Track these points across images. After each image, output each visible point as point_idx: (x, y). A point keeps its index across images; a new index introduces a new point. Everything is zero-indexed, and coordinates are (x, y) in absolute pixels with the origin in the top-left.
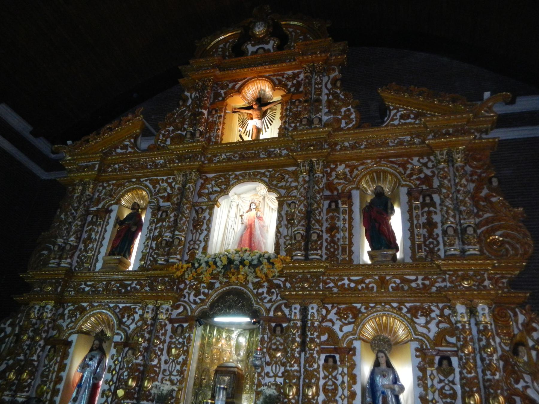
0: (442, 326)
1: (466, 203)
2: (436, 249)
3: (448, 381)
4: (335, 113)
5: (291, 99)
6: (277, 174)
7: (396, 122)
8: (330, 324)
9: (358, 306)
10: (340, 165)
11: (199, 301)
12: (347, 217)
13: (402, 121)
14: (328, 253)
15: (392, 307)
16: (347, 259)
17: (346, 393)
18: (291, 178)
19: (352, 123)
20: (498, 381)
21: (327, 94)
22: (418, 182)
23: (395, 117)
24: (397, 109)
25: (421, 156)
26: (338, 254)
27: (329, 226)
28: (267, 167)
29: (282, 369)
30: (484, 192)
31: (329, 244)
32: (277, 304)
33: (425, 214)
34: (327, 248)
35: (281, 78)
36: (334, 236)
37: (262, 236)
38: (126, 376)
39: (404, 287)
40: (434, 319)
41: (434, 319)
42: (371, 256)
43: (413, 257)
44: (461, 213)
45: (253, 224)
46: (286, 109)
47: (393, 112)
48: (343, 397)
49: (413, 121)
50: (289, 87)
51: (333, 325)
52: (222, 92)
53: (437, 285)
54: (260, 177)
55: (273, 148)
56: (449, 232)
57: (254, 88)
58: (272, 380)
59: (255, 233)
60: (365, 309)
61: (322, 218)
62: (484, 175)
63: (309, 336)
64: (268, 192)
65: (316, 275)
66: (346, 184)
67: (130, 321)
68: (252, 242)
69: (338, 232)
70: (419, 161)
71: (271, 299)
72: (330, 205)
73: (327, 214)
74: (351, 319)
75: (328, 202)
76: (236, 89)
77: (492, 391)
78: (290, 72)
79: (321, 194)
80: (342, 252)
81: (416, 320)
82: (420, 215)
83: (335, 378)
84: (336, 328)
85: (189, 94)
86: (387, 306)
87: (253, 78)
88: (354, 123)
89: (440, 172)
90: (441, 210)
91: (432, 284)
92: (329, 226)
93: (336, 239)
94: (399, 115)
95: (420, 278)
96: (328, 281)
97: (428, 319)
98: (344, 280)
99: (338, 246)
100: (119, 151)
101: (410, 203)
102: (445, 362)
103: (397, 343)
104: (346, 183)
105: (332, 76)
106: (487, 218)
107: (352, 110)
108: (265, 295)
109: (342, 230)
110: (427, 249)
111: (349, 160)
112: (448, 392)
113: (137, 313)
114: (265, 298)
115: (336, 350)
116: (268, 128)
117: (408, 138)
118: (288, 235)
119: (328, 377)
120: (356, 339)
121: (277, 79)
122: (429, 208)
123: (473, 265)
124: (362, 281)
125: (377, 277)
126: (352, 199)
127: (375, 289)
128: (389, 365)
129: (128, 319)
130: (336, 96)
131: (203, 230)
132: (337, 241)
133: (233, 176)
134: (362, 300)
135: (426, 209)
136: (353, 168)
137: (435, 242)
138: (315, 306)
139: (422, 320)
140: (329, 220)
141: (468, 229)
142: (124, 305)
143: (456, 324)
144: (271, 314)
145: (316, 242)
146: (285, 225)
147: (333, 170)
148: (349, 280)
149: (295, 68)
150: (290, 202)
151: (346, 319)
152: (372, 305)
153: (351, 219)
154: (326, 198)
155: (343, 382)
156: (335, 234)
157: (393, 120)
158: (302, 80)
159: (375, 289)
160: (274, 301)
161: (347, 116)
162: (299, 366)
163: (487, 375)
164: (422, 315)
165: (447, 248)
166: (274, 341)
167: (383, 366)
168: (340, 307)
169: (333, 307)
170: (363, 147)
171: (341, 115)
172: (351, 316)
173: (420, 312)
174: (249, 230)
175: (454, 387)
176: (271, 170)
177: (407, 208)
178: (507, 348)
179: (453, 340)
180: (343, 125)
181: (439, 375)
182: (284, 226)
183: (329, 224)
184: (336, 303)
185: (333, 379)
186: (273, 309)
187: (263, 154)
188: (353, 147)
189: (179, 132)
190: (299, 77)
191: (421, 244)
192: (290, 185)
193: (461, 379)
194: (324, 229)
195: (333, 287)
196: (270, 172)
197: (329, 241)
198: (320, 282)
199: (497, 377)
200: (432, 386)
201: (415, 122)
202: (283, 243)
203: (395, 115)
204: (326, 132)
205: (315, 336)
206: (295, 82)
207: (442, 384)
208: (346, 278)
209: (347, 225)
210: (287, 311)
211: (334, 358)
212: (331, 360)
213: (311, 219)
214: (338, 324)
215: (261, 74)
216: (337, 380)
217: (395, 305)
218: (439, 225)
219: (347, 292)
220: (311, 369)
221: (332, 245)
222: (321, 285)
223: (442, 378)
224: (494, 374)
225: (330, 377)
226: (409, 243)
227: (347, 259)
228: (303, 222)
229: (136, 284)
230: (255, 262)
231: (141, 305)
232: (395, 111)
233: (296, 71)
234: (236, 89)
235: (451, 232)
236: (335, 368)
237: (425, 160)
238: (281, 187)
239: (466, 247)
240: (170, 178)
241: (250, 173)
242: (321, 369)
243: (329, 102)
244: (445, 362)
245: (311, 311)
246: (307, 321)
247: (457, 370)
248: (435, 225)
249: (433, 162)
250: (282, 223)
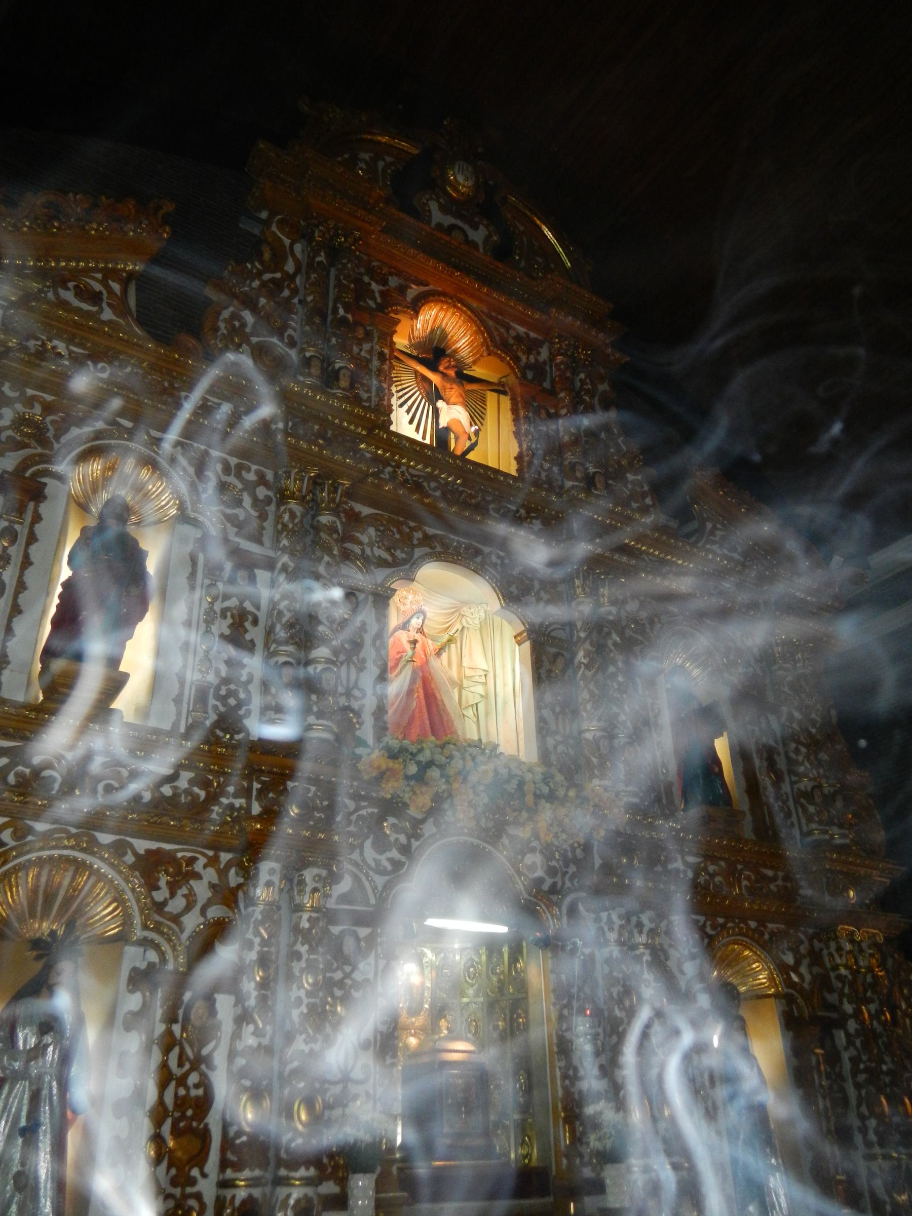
11: (389, 868)
35: (503, 330)
38: (197, 1086)
52: (374, 286)
59: (438, 696)
60: (714, 927)
64: (502, 607)
67: (177, 904)
76: (409, 299)
78: (521, 330)
85: (287, 242)
87: (444, 294)
100: (68, 295)
113: (198, 876)
129: (173, 895)
131: (364, 661)
133: (418, 535)
142: (153, 845)
171: (627, 488)
189: (275, 340)
190: (539, 353)
193: (855, 1072)
206: (532, 359)
215: (462, 296)
229: (191, 782)
231: (211, 853)
233: (533, 335)
234: (409, 299)
240: (249, 470)
247: (846, 1056)
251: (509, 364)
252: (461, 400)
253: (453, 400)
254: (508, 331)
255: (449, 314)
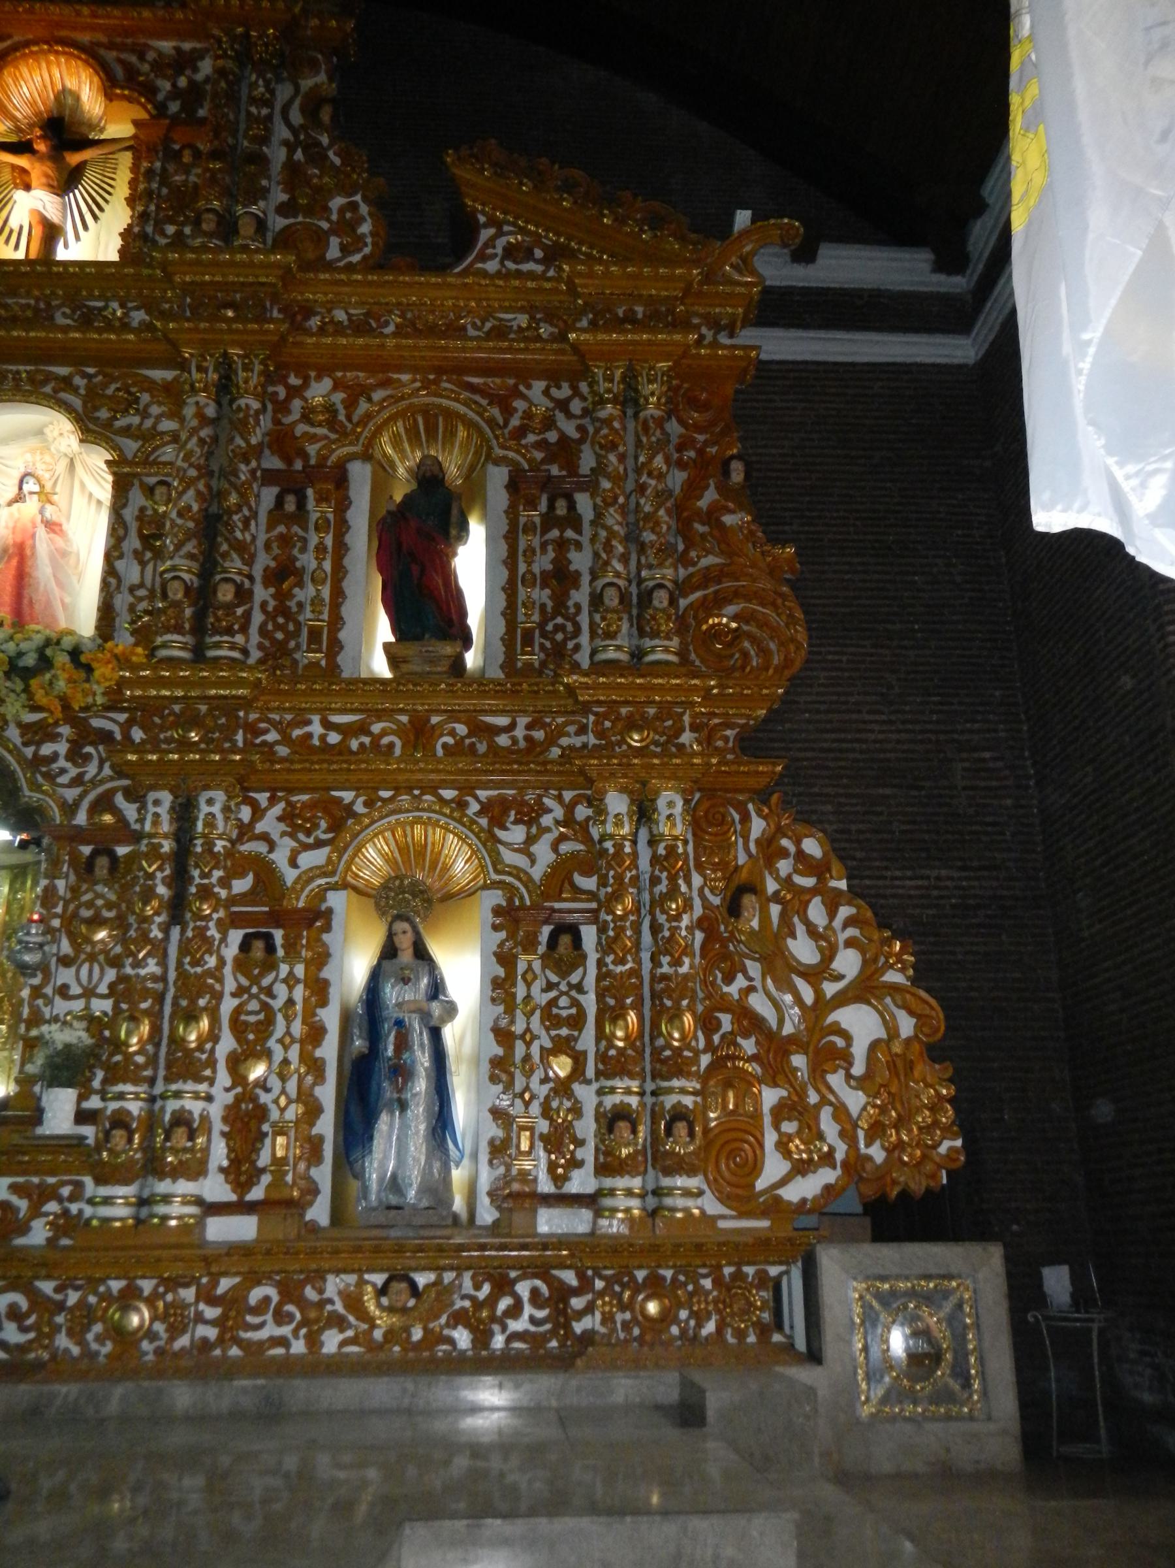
0: (565, 848)
1: (657, 523)
2: (570, 645)
3: (569, 984)
4: (309, 211)
5: (167, 140)
6: (113, 387)
7: (492, 266)
8: (262, 848)
9: (347, 796)
10: (319, 378)
12: (329, 541)
13: (510, 265)
14: (267, 643)
15: (441, 800)
16: (323, 663)
17: (297, 1028)
18: (160, 404)
19: (359, 250)
20: (686, 977)
21: (286, 143)
22: (539, 455)
23: (490, 251)
24: (498, 225)
25: (554, 376)
26: (298, 646)
27: (273, 564)
28: (78, 360)
29: (111, 975)
30: (710, 496)
31: (270, 616)
32: (100, 790)
33: (550, 548)
34: (263, 631)
35: (133, 59)
36: (289, 595)
37: (60, 584)
39: (478, 746)
40: (548, 830)
41: (548, 830)
42: (394, 660)
43: (509, 665)
44: (642, 548)
45: (29, 542)
46: (150, 173)
47: (486, 234)
48: (287, 1040)
49: (539, 268)
50: (160, 97)
51: (271, 850)
53: (564, 741)
54: (55, 391)
55: (98, 299)
56: (607, 601)
57: (38, 79)
58: (78, 1005)
60: (366, 804)
61: (254, 538)
62: (713, 450)
63: (197, 881)
64: (81, 441)
65: (228, 707)
66: (334, 442)
68: (26, 601)
69: (300, 584)
70: (546, 393)
71: (81, 776)
72: (279, 502)
73: (270, 527)
74: (325, 832)
75: (275, 490)
77: (669, 1003)
78: (166, 46)
79: (254, 464)
80: (310, 643)
81: (501, 834)
82: (538, 550)
83: (269, 992)
84: (280, 858)
86: (427, 797)
87: (36, 42)
88: (367, 250)
89: (601, 429)
90: (593, 540)
91: (551, 740)
92: (273, 564)
93: (292, 604)
94: (501, 243)
95: (523, 721)
96: (263, 725)
97: (534, 830)
98: (308, 723)
99: (298, 625)
101: (512, 513)
102: (565, 940)
103: (448, 897)
104: (333, 436)
105: (307, 84)
106: (707, 568)
107: (364, 209)
108: (62, 763)
109: (313, 580)
110: (548, 644)
111: (345, 368)
112: (564, 1013)
114: (63, 771)
115: (277, 918)
116: (86, 227)
117: (523, 320)
118: (142, 585)
119: (246, 990)
120: (334, 887)
121: (120, 61)
122: (562, 532)
123: (661, 689)
124: (362, 729)
125: (404, 719)
126: (347, 489)
127: (398, 751)
128: (421, 953)
130: (316, 155)
132: (295, 609)
134: (360, 781)
135: (555, 533)
136: (356, 393)
137: (570, 627)
138: (220, 796)
139: (516, 834)
140: (275, 545)
141: (655, 594)
143: (601, 841)
144: (81, 818)
145: (229, 608)
146: (136, 552)
147: (295, 392)
148: (327, 725)
149: (181, 35)
150: (152, 480)
151: (308, 834)
152: (385, 794)
153: (341, 548)
154: (270, 478)
155: (290, 1002)
156: (291, 589)
157: (483, 257)
158: (207, 79)
159: (398, 751)
160: (92, 781)
161: (346, 227)
162: (163, 963)
163: (661, 966)
164: (516, 822)
165: (599, 642)
166: (87, 897)
167: (406, 956)
168: (295, 799)
169: (273, 801)
170: (391, 329)
171: (328, 220)
172: (323, 824)
173: (513, 813)
174: (14, 562)
175: (580, 997)
176: (91, 370)
177: (504, 527)
178: (716, 901)
179: (588, 883)
180: (333, 252)
181: (549, 973)
182: (131, 556)
183: (274, 559)
184: (282, 790)
185: (262, 997)
186: (85, 804)
187: (64, 314)
188: (359, 327)
190: (196, 70)
191: (533, 629)
192: (154, 427)
193: (600, 978)
194: (258, 571)
195: (277, 743)
196: (89, 377)
197: (270, 609)
198: (238, 726)
199: (684, 969)
200: (528, 998)
201: (544, 272)
202: (126, 607)
203: (491, 243)
204: (276, 264)
205: (214, 880)
206: (182, 82)
207: (553, 994)
208: (316, 719)
209: (327, 565)
210: (130, 811)
211: (268, 939)
212: (259, 946)
213: (219, 539)
214: (286, 846)
215: (63, 33)
216: (273, 997)
217: (448, 794)
218: (585, 579)
219: (315, 758)
220: (199, 970)
221: (281, 620)
222: (239, 737)
223: (554, 979)
224: (677, 963)
225: (255, 990)
226: (501, 627)
227: (323, 663)
228: (190, 547)
230: (30, 660)
232: (491, 231)
233: (187, 46)
235: (612, 599)
236: (270, 965)
237: (565, 392)
238: (126, 431)
239: (648, 643)
241: (18, 372)
242: (228, 970)
243: (293, 171)
244: (565, 940)
245: (205, 809)
246: (192, 839)
247: (592, 957)
248: (574, 580)
249: (584, 399)
250: (126, 546)
251: (140, 103)
252: (44, 180)
253: (34, 184)
254: (142, 57)
255: (63, 67)
